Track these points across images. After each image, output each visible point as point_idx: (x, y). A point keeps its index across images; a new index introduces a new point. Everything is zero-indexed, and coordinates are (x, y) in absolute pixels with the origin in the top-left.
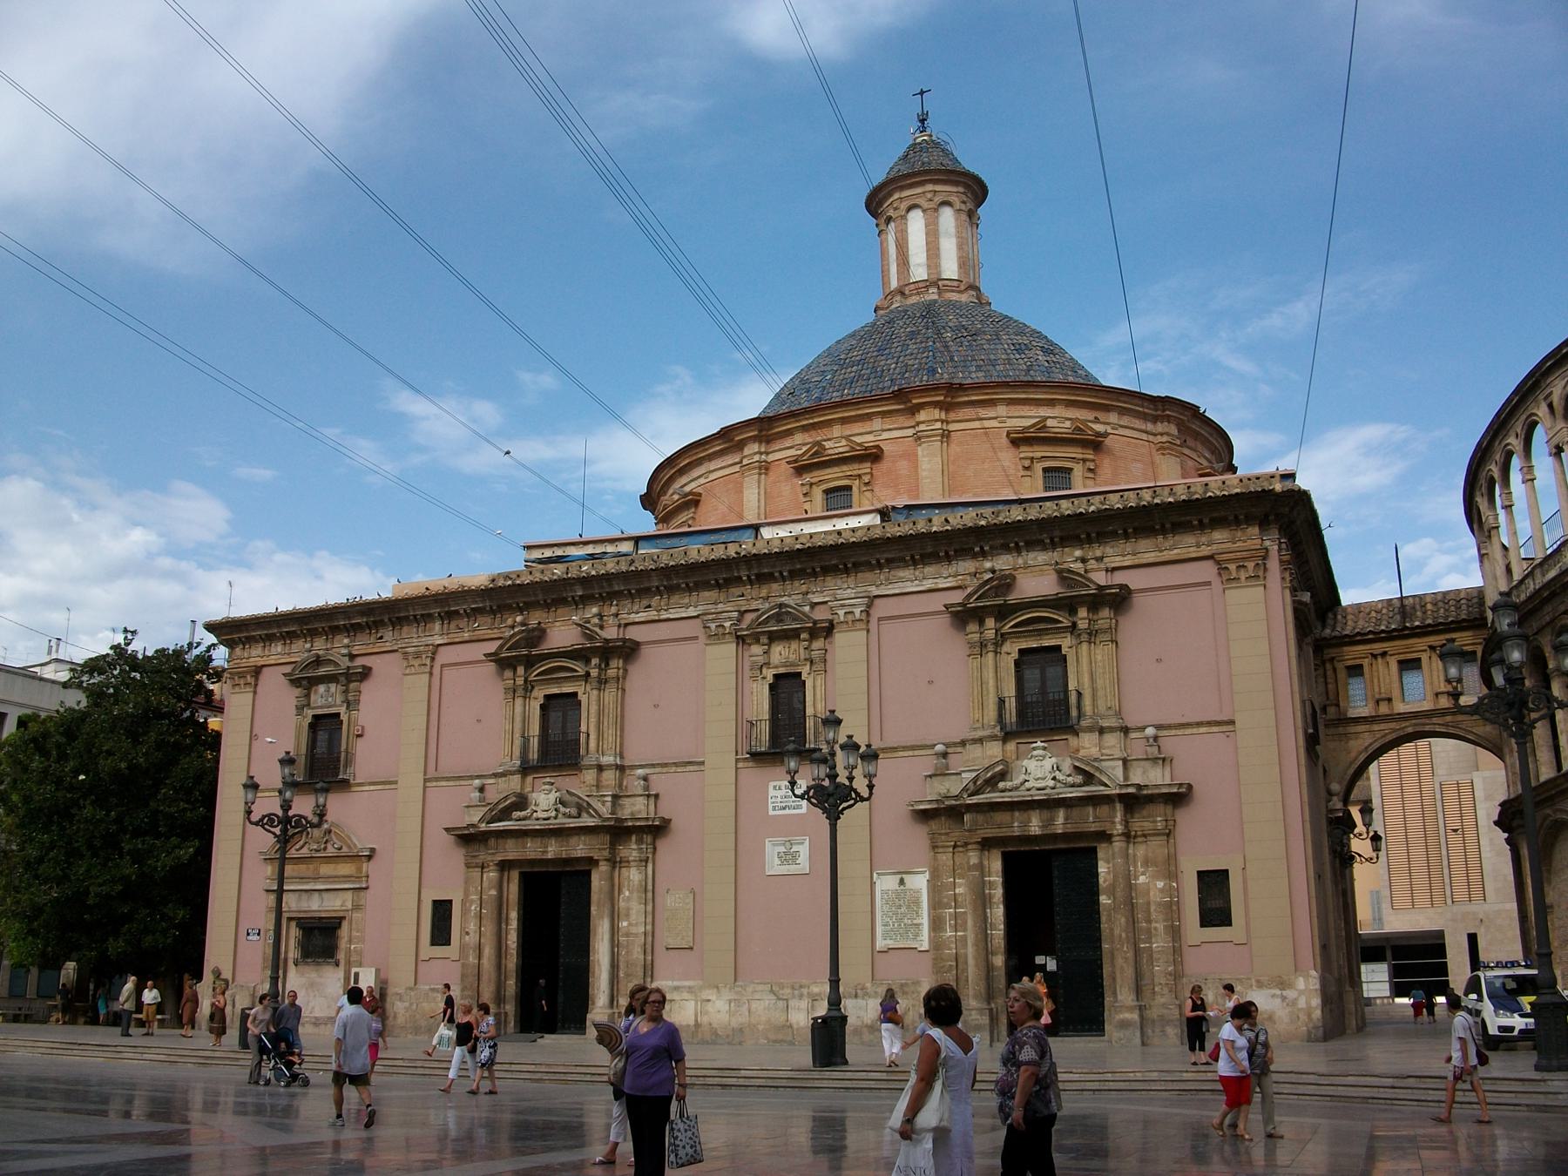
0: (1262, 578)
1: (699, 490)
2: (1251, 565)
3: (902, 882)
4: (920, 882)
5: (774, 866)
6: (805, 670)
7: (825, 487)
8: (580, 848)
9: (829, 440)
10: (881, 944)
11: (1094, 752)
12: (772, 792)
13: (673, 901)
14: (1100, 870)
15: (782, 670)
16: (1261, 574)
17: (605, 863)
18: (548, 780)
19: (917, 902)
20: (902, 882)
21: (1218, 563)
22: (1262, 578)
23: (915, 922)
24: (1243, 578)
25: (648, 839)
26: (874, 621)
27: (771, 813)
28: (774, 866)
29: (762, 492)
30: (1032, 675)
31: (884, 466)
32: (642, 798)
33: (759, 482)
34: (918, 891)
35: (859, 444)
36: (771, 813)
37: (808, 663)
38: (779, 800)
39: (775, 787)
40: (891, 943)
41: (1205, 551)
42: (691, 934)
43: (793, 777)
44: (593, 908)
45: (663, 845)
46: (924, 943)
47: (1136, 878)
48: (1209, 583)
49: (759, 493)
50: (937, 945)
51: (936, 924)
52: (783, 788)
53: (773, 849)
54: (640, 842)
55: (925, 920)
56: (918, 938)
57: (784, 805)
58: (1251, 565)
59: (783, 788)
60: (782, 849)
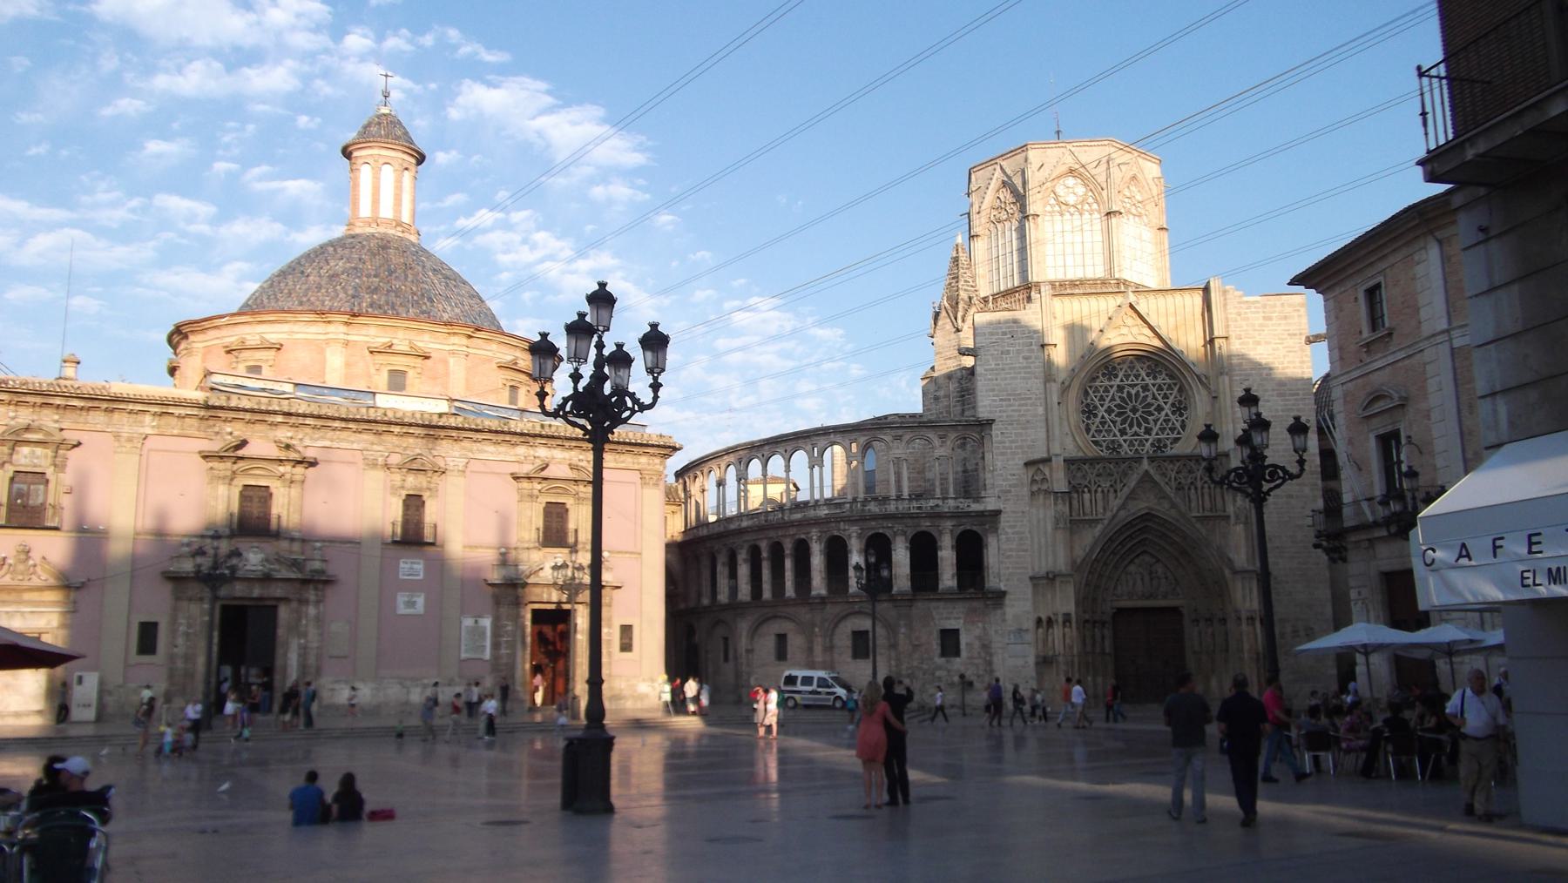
2: (655, 478)
3: (476, 622)
4: (487, 622)
5: (402, 610)
6: (426, 495)
8: (277, 591)
10: (464, 655)
12: (402, 565)
13: (338, 627)
15: (411, 493)
18: (255, 544)
19: (483, 634)
20: (476, 622)
21: (641, 474)
25: (320, 586)
26: (468, 473)
27: (401, 577)
28: (402, 610)
34: (485, 628)
36: (401, 577)
41: (636, 467)
44: (281, 632)
45: (330, 592)
46: (487, 655)
48: (635, 483)
50: (496, 657)
51: (496, 646)
53: (401, 599)
54: (316, 589)
55: (488, 643)
58: (655, 478)
60: (406, 599)
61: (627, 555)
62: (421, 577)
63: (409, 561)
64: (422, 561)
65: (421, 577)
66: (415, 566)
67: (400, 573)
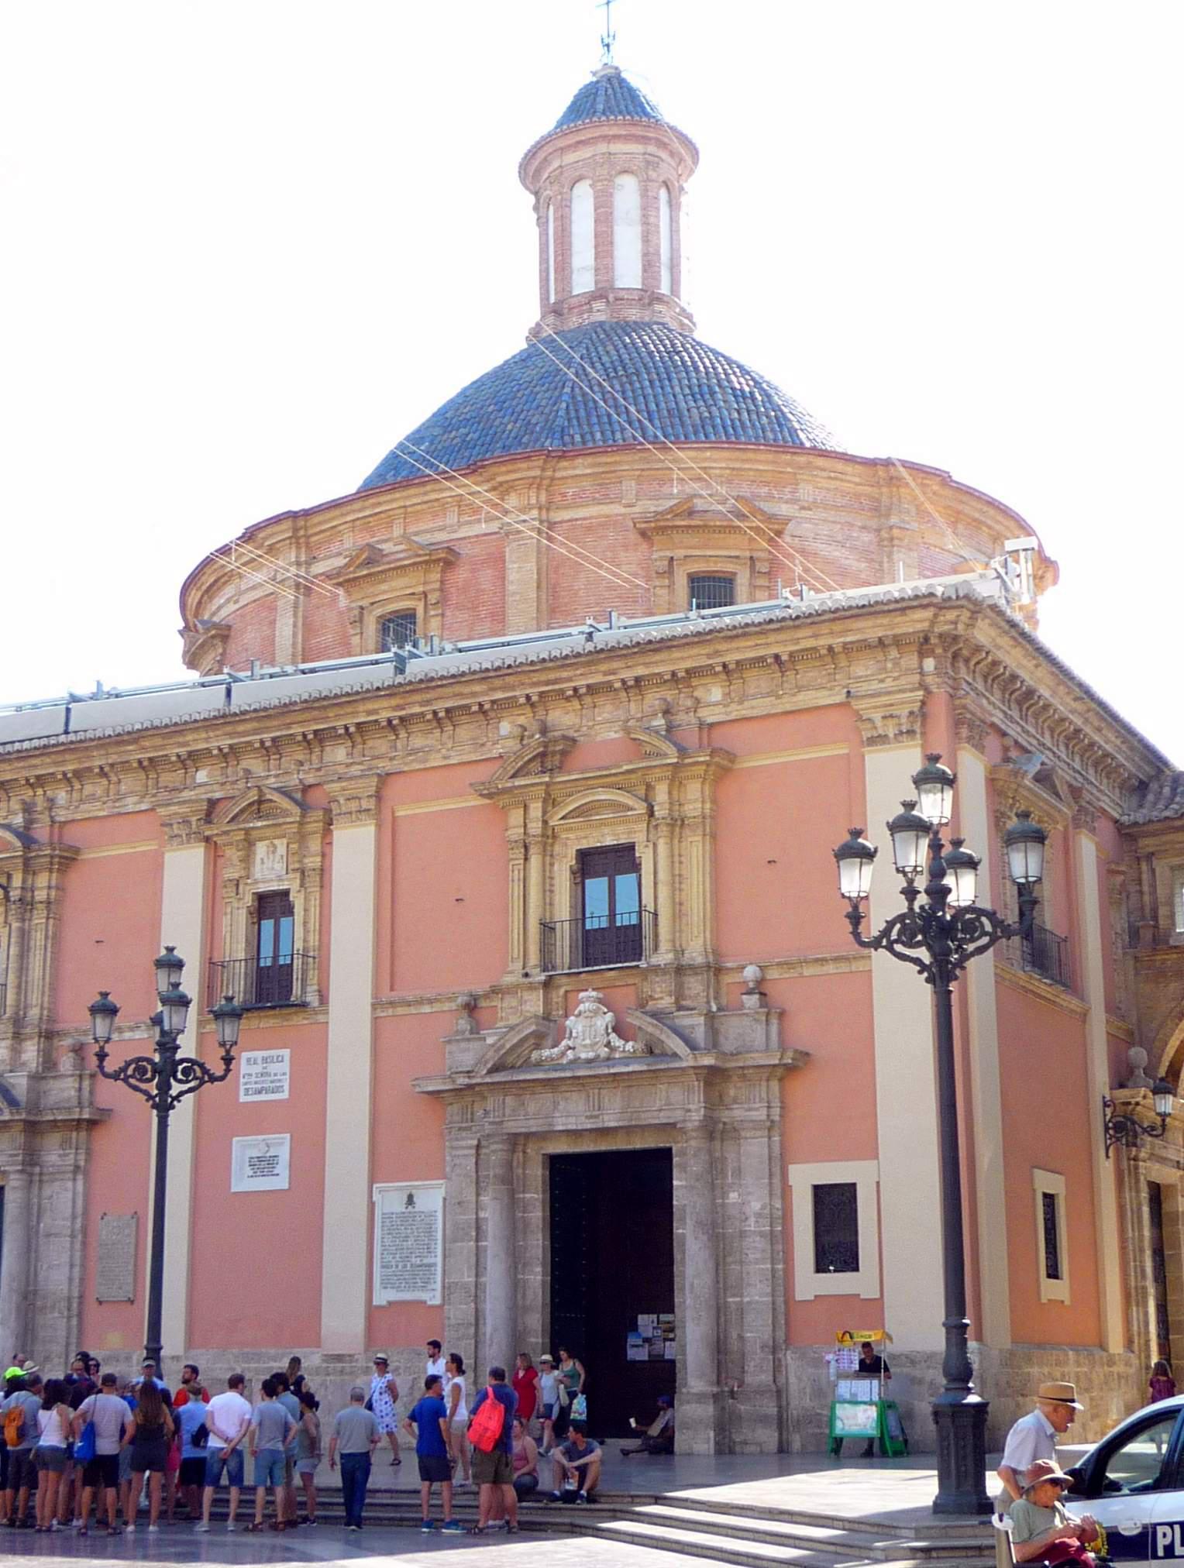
0: (918, 736)
1: (230, 621)
3: (410, 1200)
7: (379, 611)
9: (385, 541)
10: (381, 1298)
11: (666, 1002)
14: (675, 1183)
16: (917, 727)
17: (17, 1176)
19: (430, 1231)
20: (410, 1200)
22: (918, 736)
23: (425, 1261)
24: (891, 735)
27: (243, 1099)
28: (243, 1181)
29: (300, 624)
30: (597, 887)
31: (461, 575)
32: (70, 1079)
33: (296, 606)
34: (432, 1214)
35: (422, 547)
36: (243, 1099)
37: (298, 875)
38: (253, 1079)
39: (249, 1060)
40: (392, 1295)
42: (130, 1279)
43: (228, 1052)
47: (724, 1195)
49: (295, 626)
52: (259, 1061)
53: (243, 1148)
56: (430, 1287)
57: (259, 1086)
59: (259, 1061)
61: (831, 968)
62: (285, 1095)
63: (259, 1054)
64: (286, 1053)
65: (285, 1095)
66: (273, 1068)
67: (242, 1088)
